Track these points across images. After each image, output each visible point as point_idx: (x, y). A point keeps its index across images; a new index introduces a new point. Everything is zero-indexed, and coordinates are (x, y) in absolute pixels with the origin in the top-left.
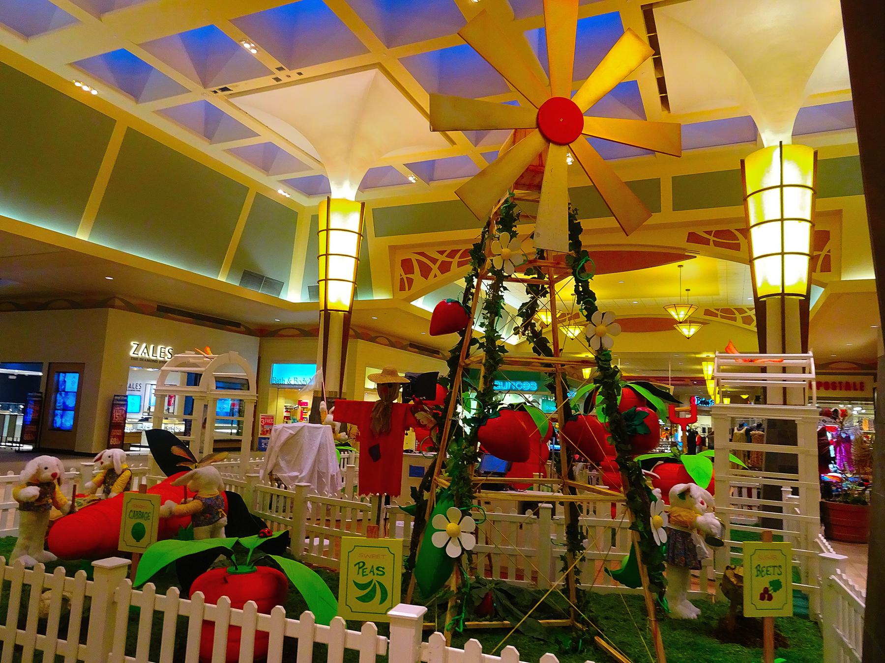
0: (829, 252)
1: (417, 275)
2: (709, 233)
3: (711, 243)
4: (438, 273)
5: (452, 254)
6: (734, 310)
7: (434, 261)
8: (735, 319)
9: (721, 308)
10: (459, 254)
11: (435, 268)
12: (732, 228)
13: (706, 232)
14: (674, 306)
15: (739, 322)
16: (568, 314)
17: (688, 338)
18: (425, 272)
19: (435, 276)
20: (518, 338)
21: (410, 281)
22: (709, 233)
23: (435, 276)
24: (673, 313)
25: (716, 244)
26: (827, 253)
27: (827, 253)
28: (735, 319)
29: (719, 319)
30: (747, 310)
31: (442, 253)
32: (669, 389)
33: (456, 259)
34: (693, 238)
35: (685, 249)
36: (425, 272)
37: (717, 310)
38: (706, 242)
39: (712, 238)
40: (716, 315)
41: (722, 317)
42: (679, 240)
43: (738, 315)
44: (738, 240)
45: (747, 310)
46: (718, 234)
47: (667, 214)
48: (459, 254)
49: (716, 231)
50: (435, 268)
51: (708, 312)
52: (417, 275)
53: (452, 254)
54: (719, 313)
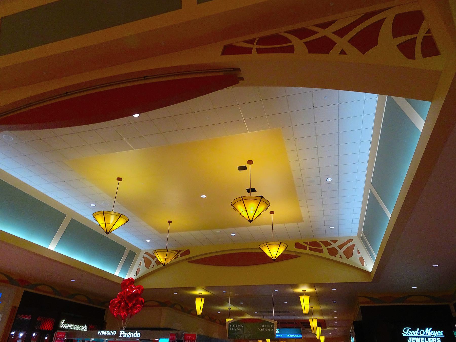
0: (429, 32)
2: (251, 42)
8: (322, 251)
9: (309, 241)
15: (326, 254)
16: (180, 251)
25: (259, 51)
26: (427, 35)
27: (427, 35)
28: (322, 251)
29: (308, 251)
30: (331, 243)
32: (273, 324)
37: (306, 243)
40: (305, 248)
41: (311, 249)
43: (325, 248)
44: (291, 42)
45: (331, 243)
51: (298, 245)
54: (308, 246)
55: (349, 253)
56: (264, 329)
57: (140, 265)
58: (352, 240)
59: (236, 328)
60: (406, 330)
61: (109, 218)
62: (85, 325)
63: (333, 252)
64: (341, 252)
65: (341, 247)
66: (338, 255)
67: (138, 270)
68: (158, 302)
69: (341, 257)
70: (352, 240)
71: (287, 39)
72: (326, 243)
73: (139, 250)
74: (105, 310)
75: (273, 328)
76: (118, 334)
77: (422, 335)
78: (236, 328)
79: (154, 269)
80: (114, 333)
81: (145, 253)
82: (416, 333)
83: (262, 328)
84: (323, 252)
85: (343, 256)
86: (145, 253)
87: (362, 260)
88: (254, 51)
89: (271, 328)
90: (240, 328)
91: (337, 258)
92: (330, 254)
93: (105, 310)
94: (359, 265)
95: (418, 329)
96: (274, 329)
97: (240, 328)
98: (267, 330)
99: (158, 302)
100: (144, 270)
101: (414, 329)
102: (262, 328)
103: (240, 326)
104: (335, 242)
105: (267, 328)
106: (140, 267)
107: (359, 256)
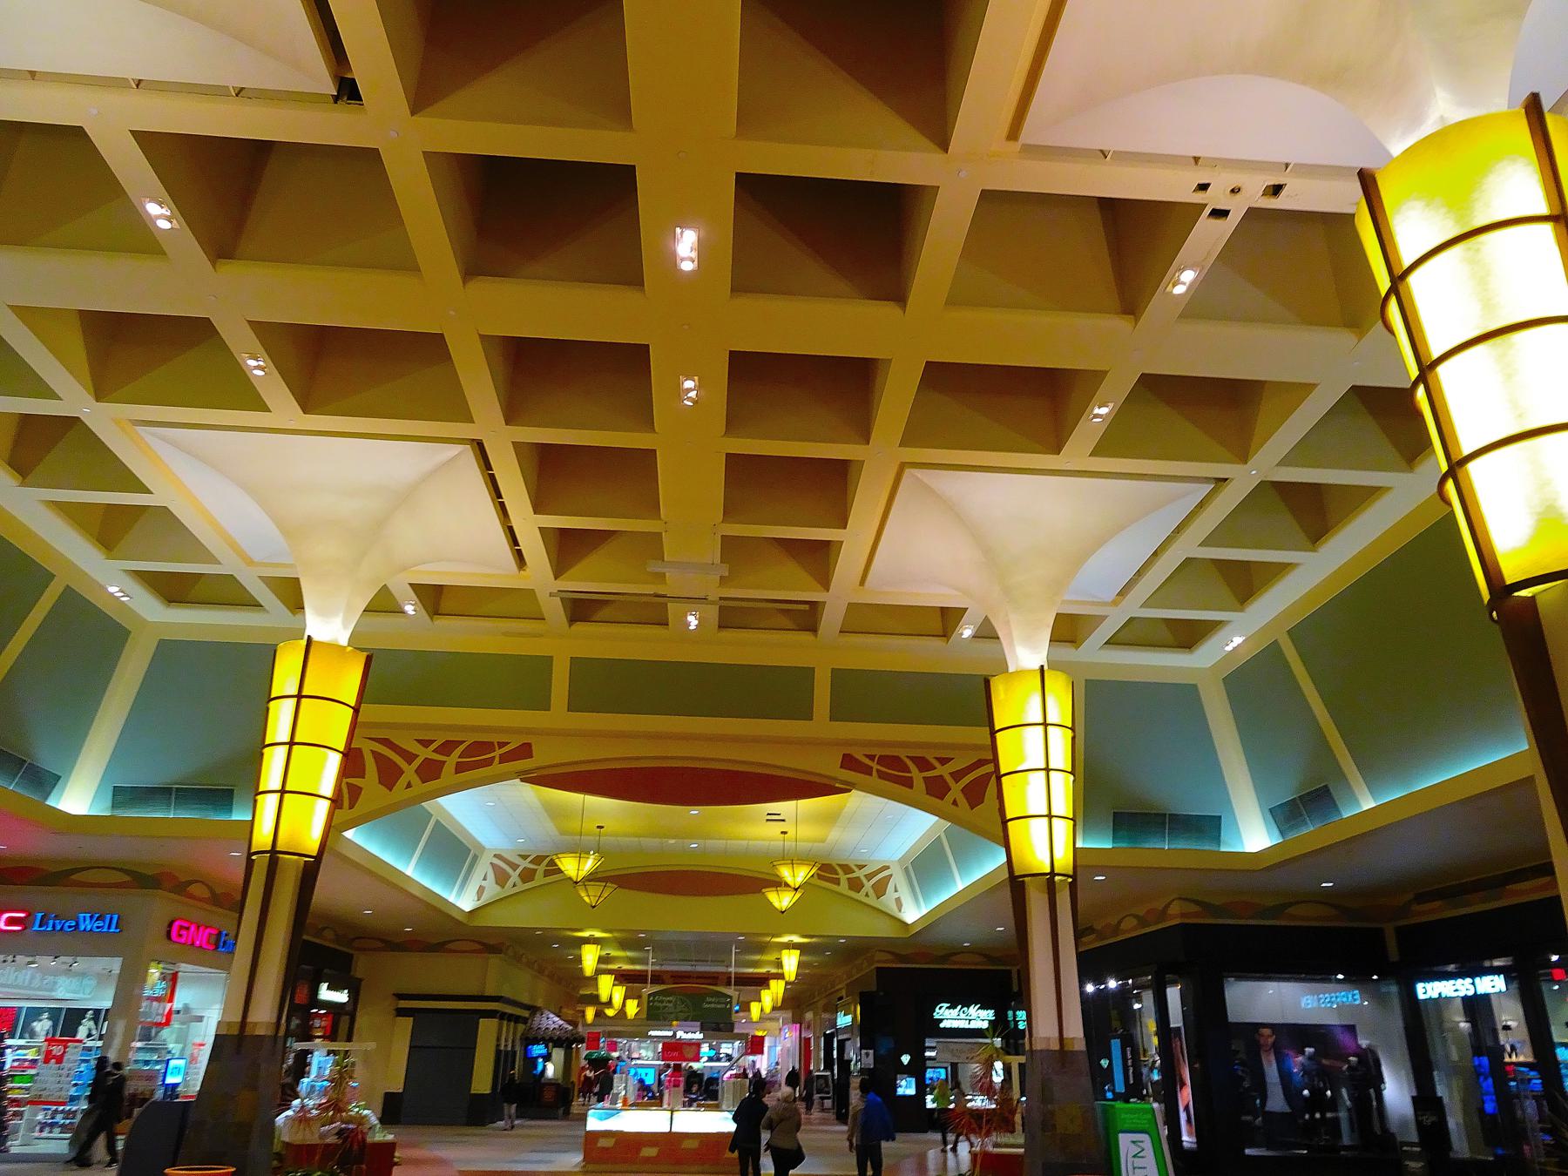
1: (370, 780)
2: (871, 757)
3: (874, 773)
4: (416, 780)
5: (447, 747)
6: (838, 868)
7: (409, 757)
8: (837, 882)
10: (462, 747)
11: (409, 771)
12: (902, 754)
13: (867, 756)
14: (790, 861)
15: (843, 888)
17: (783, 912)
18: (390, 777)
19: (409, 785)
20: (476, 899)
21: (355, 792)
22: (871, 757)
23: (409, 785)
24: (785, 873)
25: (882, 775)
28: (837, 882)
31: (426, 743)
32: (731, 997)
33: (452, 760)
34: (849, 762)
35: (835, 779)
36: (390, 777)
38: (867, 771)
39: (875, 766)
42: (828, 765)
43: (843, 878)
46: (883, 760)
47: (821, 724)
48: (462, 747)
49: (880, 756)
50: (409, 771)
52: (370, 780)
53: (447, 747)
55: (880, 889)
56: (713, 1006)
57: (485, 879)
58: (888, 868)
59: (662, 1002)
60: (940, 1008)
61: (586, 862)
62: (346, 991)
63: (856, 885)
64: (868, 885)
65: (869, 877)
66: (863, 891)
67: (481, 890)
68: (479, 943)
69: (867, 895)
70: (888, 868)
71: (908, 768)
72: (847, 869)
73: (482, 848)
74: (352, 955)
75: (731, 1002)
76: (675, 1034)
77: (962, 1016)
78: (662, 1002)
79: (516, 890)
80: (670, 1033)
81: (495, 856)
82: (954, 1013)
83: (710, 1003)
84: (839, 884)
85: (871, 892)
86: (495, 856)
87: (898, 902)
88: (874, 773)
89: (726, 1004)
90: (670, 1002)
91: (860, 896)
92: (851, 888)
93: (352, 955)
94: (893, 910)
95: (960, 1006)
96: (731, 1006)
97: (670, 1002)
98: (719, 1006)
99: (479, 943)
100: (492, 891)
101: (953, 1007)
102: (710, 1003)
103: (671, 998)
104: (861, 867)
105: (719, 1003)
106: (484, 883)
107: (896, 895)
